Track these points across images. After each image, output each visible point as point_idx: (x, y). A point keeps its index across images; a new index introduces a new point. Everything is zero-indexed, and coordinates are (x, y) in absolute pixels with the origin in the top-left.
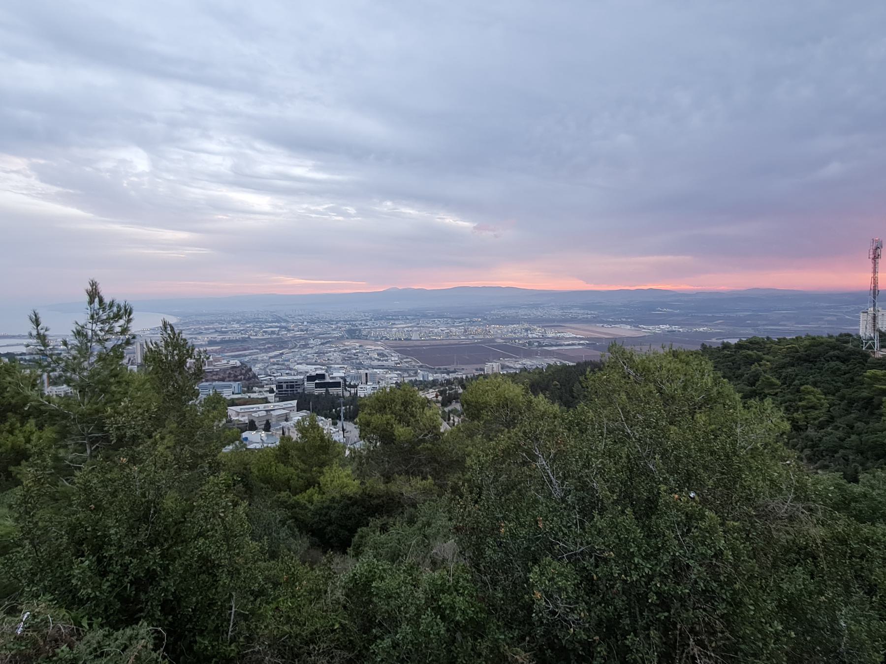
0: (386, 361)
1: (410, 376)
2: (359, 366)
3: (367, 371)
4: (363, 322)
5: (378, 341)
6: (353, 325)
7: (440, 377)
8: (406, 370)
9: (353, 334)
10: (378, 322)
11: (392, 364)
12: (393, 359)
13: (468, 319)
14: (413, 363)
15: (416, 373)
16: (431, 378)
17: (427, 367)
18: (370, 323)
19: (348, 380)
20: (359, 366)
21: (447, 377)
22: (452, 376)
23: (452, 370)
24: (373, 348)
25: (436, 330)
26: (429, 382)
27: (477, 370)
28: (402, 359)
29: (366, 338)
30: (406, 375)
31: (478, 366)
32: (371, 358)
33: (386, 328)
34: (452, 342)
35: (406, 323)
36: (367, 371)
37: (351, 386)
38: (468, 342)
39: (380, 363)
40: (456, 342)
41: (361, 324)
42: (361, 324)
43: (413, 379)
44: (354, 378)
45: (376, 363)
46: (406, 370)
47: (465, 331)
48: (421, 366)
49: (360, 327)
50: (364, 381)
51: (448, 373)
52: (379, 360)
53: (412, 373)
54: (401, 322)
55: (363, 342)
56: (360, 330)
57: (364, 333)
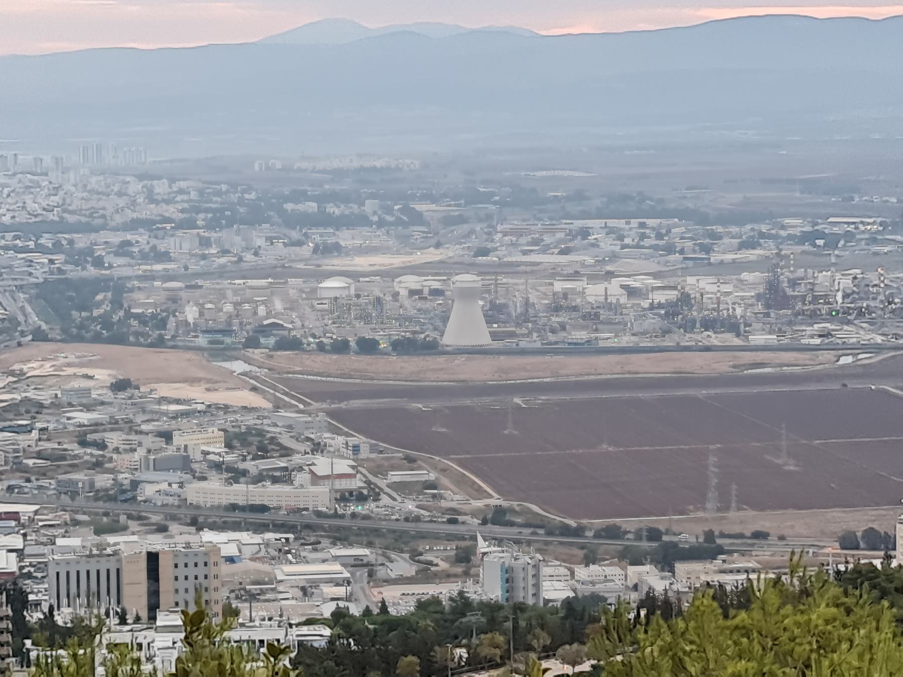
0: (283, 477)
1: (426, 574)
2: (118, 506)
3: (156, 542)
4: (141, 239)
5: (219, 351)
6: (80, 257)
7: (615, 581)
8: (400, 538)
9: (78, 310)
10: (233, 238)
11: (320, 498)
12: (322, 465)
13: (797, 225)
14: (453, 498)
15: (465, 558)
16: (556, 589)
17: (536, 523)
18: (180, 244)
19: (40, 593)
20: (118, 506)
21: (656, 581)
22: (691, 575)
23: (688, 537)
24: (199, 395)
25: (594, 292)
26: (542, 616)
27: (848, 542)
28: (380, 470)
29: (156, 331)
30: (402, 566)
31: (858, 520)
32: (184, 463)
33: (280, 272)
34: (697, 363)
35: (406, 244)
36: (156, 542)
37: (53, 635)
38: (793, 362)
39: (241, 493)
40: (721, 364)
41: (123, 249)
42: (123, 249)
43: (445, 591)
44: (68, 585)
45: (213, 491)
46: (400, 538)
47: (774, 297)
48: (498, 517)
49: (120, 267)
50: (136, 602)
51: (667, 558)
52: (236, 475)
53: (439, 557)
54: (380, 237)
55: (134, 360)
56: (119, 288)
57: (144, 302)
